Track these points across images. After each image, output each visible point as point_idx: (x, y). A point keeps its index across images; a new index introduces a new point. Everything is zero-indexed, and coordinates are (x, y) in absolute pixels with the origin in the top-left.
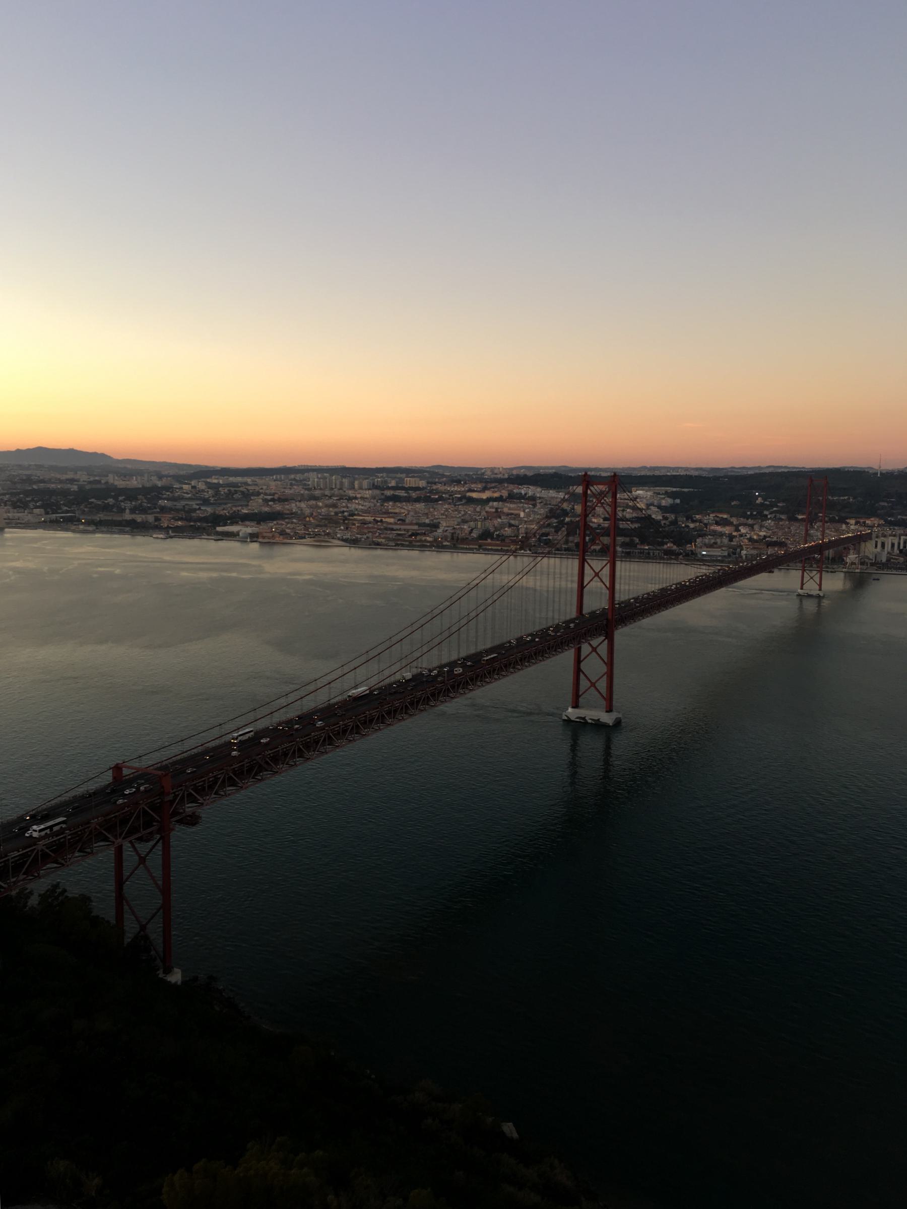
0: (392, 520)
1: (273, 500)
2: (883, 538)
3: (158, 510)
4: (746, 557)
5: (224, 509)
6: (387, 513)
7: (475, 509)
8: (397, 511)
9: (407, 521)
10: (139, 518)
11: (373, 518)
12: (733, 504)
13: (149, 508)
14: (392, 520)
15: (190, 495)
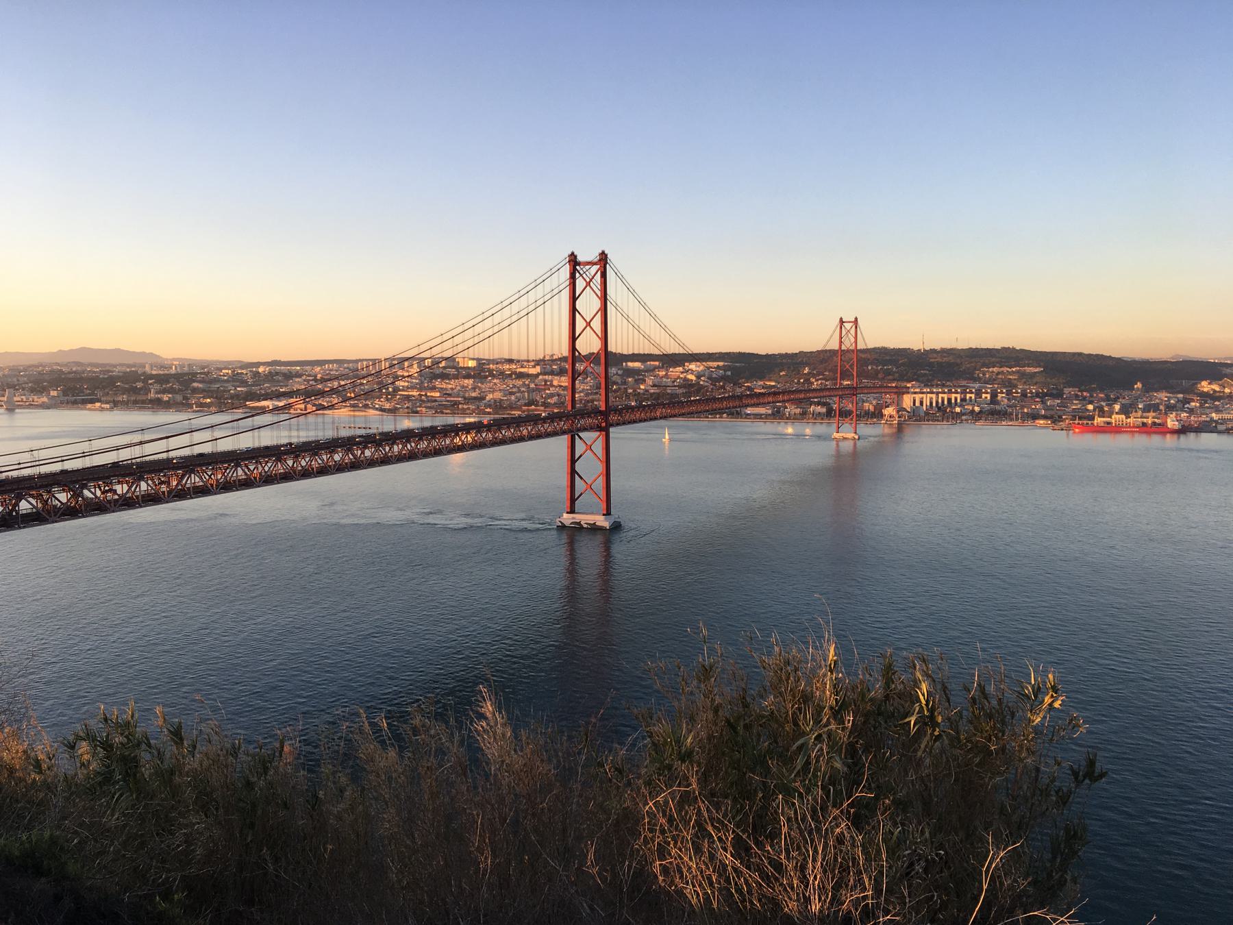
0: (438, 394)
1: (316, 380)
2: (921, 395)
3: (190, 391)
4: (789, 414)
5: (261, 389)
6: (434, 389)
7: (524, 383)
8: (444, 386)
9: (453, 395)
10: (165, 398)
11: (418, 393)
12: (781, 374)
13: (180, 390)
14: (438, 394)
15: (226, 378)
